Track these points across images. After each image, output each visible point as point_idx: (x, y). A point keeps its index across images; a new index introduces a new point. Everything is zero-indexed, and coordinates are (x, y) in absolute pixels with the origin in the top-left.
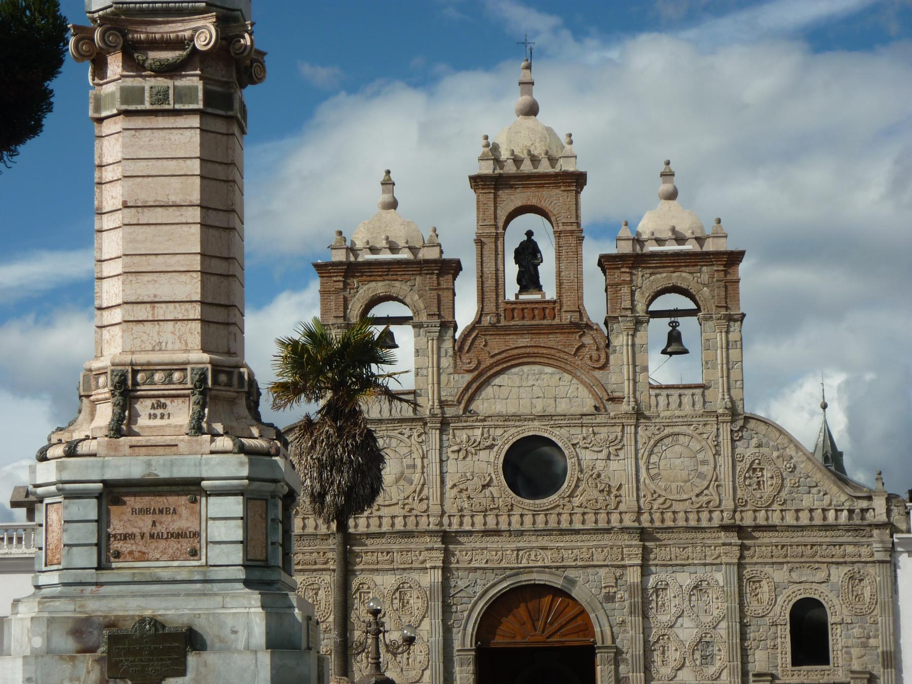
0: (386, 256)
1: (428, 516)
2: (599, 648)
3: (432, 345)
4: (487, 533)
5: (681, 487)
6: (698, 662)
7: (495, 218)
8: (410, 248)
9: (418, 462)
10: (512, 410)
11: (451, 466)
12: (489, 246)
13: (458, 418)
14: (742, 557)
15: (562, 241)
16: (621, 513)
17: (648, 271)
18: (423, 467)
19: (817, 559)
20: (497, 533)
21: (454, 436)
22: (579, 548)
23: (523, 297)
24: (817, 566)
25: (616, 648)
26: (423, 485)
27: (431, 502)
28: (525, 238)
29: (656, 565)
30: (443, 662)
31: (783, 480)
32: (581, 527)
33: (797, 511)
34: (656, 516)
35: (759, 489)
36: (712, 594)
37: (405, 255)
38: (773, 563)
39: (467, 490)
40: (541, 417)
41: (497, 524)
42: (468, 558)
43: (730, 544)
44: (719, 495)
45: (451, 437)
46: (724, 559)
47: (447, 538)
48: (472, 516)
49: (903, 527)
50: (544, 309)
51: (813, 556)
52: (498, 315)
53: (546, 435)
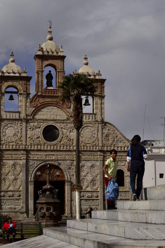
0: (12, 75)
1: (22, 145)
2: (66, 181)
3: (24, 100)
4: (38, 150)
5: (89, 140)
6: (92, 185)
7: (42, 66)
8: (19, 73)
9: (20, 131)
10: (45, 117)
11: (28, 132)
12: (40, 73)
13: (31, 119)
14: (104, 159)
15: (60, 74)
16: (73, 146)
18: (21, 132)
19: (122, 159)
20: (40, 150)
21: (30, 124)
22: (62, 155)
23: (48, 88)
24: (122, 161)
25: (71, 181)
26: (21, 137)
27: (23, 142)
28: (49, 72)
29: (82, 160)
30: (26, 184)
31: (114, 139)
32: (63, 149)
33: (118, 147)
34: (82, 147)
35: (108, 141)
36: (96, 168)
37: (17, 75)
39: (33, 139)
40: (53, 120)
41: (41, 148)
42: (33, 157)
43: (101, 155)
44: (98, 142)
45: (29, 124)
46: (99, 159)
47: (28, 152)
48: (34, 146)
50: (54, 91)
51: (122, 159)
52: (42, 92)
53: (54, 125)
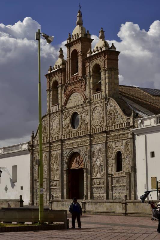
14: (107, 140)
17: (92, 61)
29: (93, 144)
38: (112, 141)
49: (136, 127)
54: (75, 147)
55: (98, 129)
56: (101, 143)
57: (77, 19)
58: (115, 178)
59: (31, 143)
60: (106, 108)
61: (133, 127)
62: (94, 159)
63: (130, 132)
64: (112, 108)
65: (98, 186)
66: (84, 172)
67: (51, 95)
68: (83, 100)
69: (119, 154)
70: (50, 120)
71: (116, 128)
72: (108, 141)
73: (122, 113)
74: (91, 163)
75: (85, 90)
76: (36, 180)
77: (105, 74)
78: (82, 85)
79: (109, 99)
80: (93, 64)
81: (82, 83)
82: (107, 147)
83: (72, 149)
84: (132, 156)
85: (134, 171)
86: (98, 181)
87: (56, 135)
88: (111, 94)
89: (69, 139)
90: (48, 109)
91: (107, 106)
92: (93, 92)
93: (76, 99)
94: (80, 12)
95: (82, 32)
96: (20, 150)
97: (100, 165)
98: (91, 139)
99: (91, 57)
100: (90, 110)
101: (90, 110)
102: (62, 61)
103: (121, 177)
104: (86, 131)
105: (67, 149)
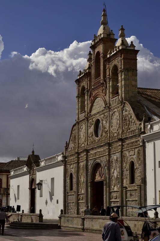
14: (122, 149)
17: (111, 62)
38: (127, 150)
54: (97, 157)
55: (116, 136)
56: (118, 152)
57: (101, 18)
58: (129, 191)
59: (64, 153)
60: (122, 113)
61: (144, 133)
62: (112, 170)
63: (141, 139)
64: (127, 113)
65: (115, 200)
66: (104, 185)
67: (80, 102)
68: (104, 106)
69: (132, 164)
70: (78, 129)
71: (130, 136)
72: (123, 150)
73: (135, 118)
74: (109, 174)
75: (105, 95)
76: (68, 194)
77: (122, 76)
78: (103, 89)
79: (124, 103)
80: (111, 66)
81: (103, 87)
82: (122, 156)
83: (95, 159)
84: (143, 165)
85: (144, 184)
86: (115, 195)
87: (83, 145)
88: (128, 97)
89: (92, 149)
90: (77, 117)
91: (123, 111)
92: (112, 96)
93: (99, 105)
94: (104, 10)
95: (104, 31)
96: (57, 161)
97: (117, 177)
98: (110, 147)
99: (110, 57)
100: (109, 116)
101: (109, 116)
102: (89, 65)
103: (134, 190)
104: (106, 139)
105: (91, 159)
